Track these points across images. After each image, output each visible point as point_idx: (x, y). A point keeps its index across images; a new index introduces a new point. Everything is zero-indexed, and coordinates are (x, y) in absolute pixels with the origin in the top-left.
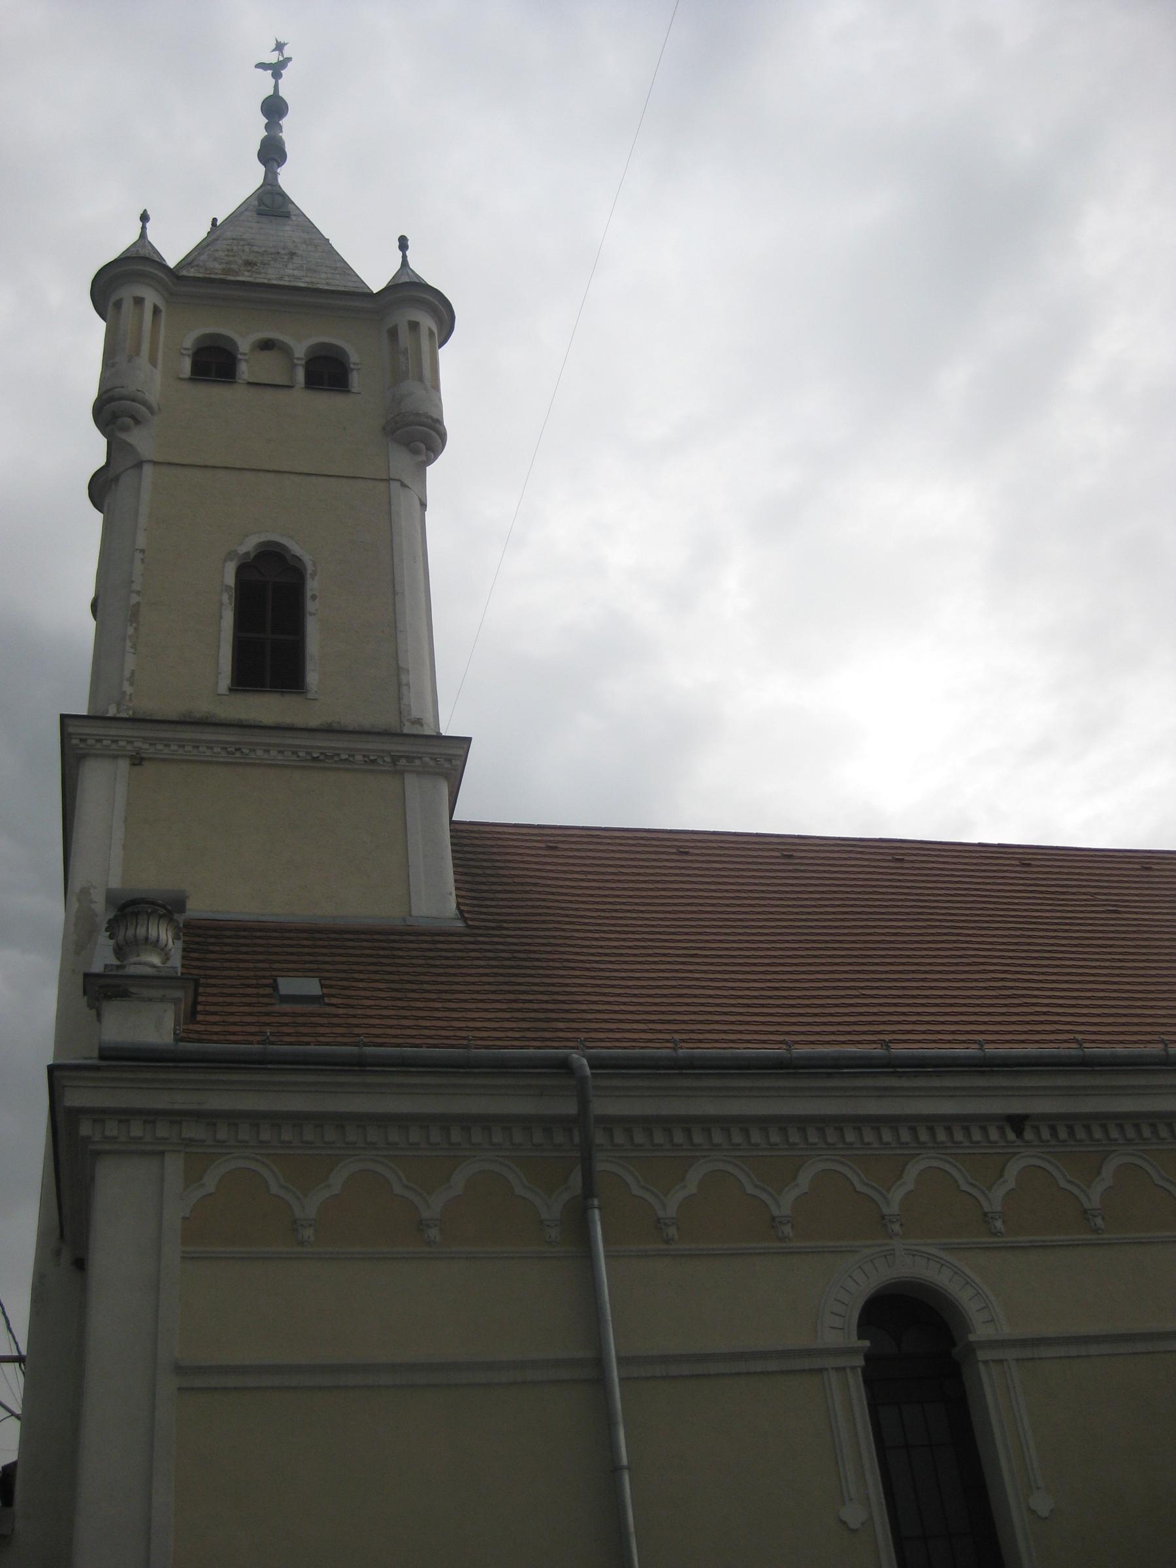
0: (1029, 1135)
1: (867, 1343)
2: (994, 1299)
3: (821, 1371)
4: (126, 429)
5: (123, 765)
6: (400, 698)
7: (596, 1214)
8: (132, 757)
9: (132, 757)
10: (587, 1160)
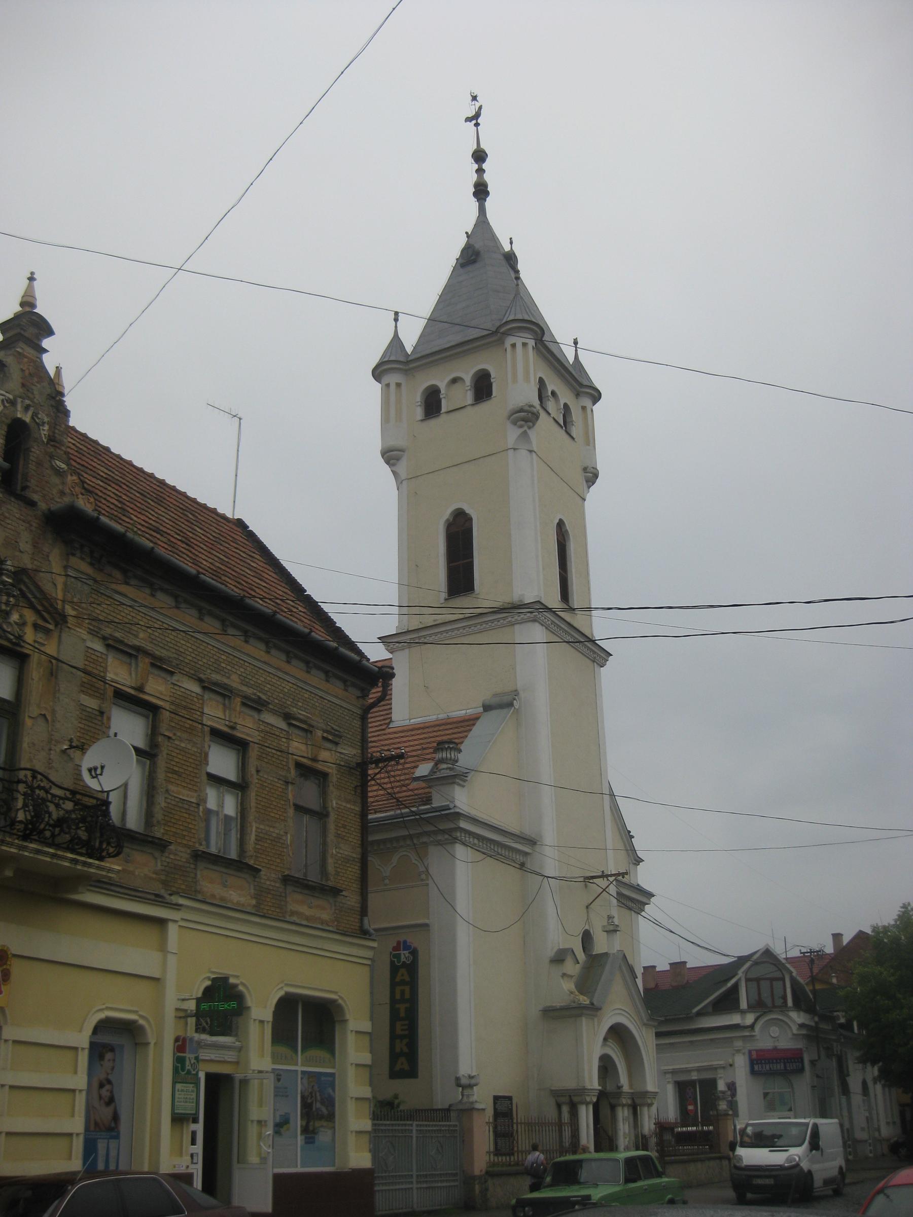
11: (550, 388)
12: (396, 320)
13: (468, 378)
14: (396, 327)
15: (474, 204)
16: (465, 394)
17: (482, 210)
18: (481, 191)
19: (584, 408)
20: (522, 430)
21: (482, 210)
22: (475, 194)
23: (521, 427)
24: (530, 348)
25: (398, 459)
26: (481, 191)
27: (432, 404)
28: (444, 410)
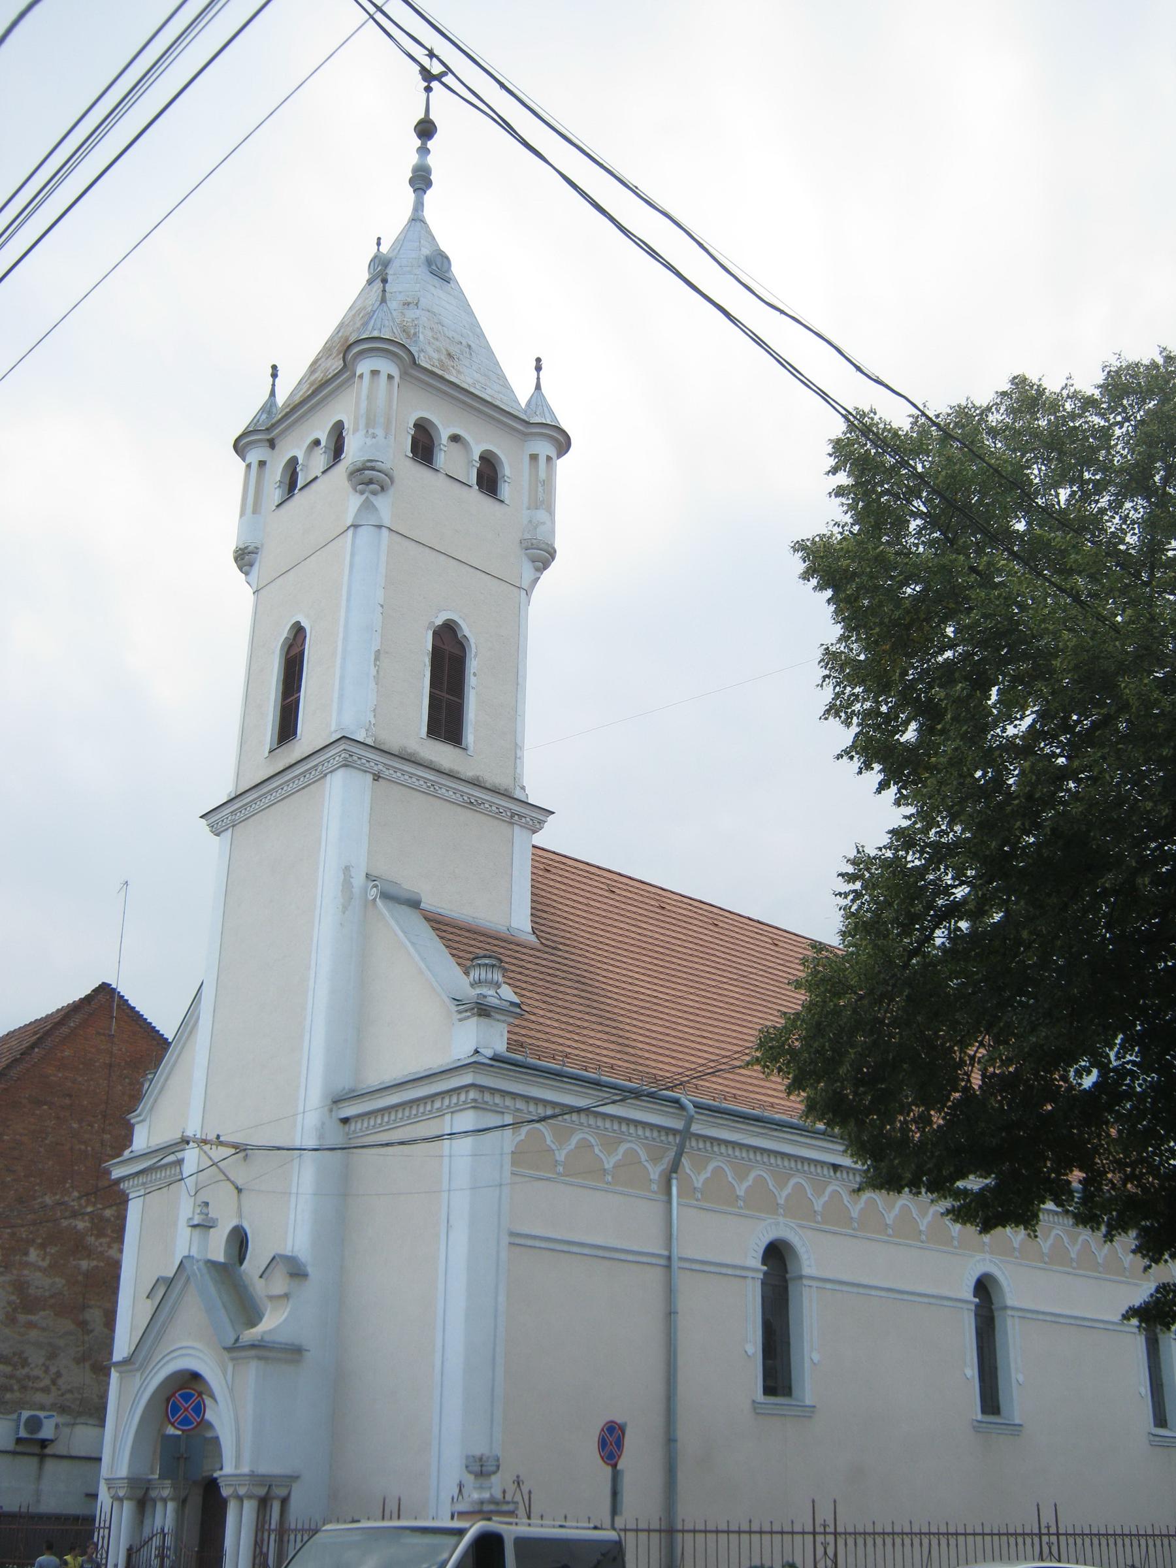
0: (838, 1174)
1: (765, 1268)
2: (815, 1257)
3: (745, 1277)
4: (374, 493)
5: (370, 777)
6: (515, 768)
7: (674, 1182)
8: (374, 774)
9: (374, 774)
10: (679, 1154)
11: (444, 434)
12: (274, 375)
14: (273, 385)
15: (409, 195)
16: (320, 459)
17: (419, 206)
18: (421, 180)
19: (534, 458)
20: (364, 497)
21: (419, 206)
22: (412, 182)
23: (362, 493)
24: (383, 378)
25: (251, 565)
26: (421, 180)
27: (291, 485)
28: (299, 485)
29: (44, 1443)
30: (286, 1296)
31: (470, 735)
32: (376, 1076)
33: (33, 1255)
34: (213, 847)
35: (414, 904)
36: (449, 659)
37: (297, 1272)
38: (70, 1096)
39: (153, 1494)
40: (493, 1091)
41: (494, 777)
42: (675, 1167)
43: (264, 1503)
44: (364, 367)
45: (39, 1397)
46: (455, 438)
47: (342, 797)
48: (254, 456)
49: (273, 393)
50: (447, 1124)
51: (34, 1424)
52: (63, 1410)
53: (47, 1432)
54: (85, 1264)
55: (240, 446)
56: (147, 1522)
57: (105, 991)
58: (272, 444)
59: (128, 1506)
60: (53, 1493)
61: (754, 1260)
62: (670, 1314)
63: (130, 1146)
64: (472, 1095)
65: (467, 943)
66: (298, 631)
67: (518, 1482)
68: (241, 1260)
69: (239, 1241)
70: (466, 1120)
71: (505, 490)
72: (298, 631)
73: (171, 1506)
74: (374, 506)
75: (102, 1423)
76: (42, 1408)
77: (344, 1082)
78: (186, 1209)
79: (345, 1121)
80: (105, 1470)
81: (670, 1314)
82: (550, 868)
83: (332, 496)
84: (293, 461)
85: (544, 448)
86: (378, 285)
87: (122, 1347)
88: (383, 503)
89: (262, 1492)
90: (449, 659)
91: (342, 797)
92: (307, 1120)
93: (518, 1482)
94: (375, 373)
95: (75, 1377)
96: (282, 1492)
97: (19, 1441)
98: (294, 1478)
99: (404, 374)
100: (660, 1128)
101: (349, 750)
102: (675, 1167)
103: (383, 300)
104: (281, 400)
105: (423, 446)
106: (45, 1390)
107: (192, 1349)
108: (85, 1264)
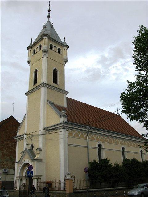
12: (32, 40)
13: (39, 47)
16: (38, 49)
17: (49, 20)
21: (49, 20)
24: (46, 39)
25: (30, 63)
26: (49, 17)
29: (6, 172)
30: (39, 153)
31: (58, 83)
32: (49, 126)
33: (4, 149)
34: (26, 98)
35: (53, 103)
36: (55, 73)
37: (40, 150)
38: (8, 130)
39: (22, 178)
40: (65, 126)
41: (61, 88)
42: (88, 135)
43: (38, 179)
44: (44, 38)
45: (5, 167)
46: (55, 47)
47: (43, 90)
48: (30, 50)
49: (32, 42)
50: (60, 130)
51: (5, 170)
52: (9, 168)
53: (7, 171)
54: (10, 150)
55: (28, 49)
56: (22, 182)
57: (12, 117)
58: (32, 48)
59: (19, 180)
60: (8, 179)
61: (97, 146)
62: (88, 153)
63: (16, 135)
64: (63, 127)
65: (59, 108)
66: (36, 70)
67: (73, 175)
68: (33, 148)
69: (32, 146)
70: (63, 130)
71: (61, 53)
72: (36, 70)
73: (25, 180)
74: (46, 55)
75: (14, 169)
76: (6, 168)
77: (45, 126)
78: (25, 143)
79: (45, 131)
80: (16, 175)
81: (88, 153)
82: (68, 99)
83: (40, 54)
84: (35, 50)
85: (65, 48)
86: (45, 28)
87: (17, 160)
88: (47, 55)
89: (38, 178)
90: (55, 73)
91: (43, 90)
92: (41, 131)
93: (73, 175)
94: (45, 38)
95: (10, 164)
96: (40, 178)
97: (3, 172)
98: (41, 176)
99: (49, 39)
100: (86, 131)
101: (44, 85)
102: (88, 135)
103: (46, 30)
104: (33, 43)
105: (51, 47)
106: (6, 166)
107: (27, 160)
108: (10, 150)
